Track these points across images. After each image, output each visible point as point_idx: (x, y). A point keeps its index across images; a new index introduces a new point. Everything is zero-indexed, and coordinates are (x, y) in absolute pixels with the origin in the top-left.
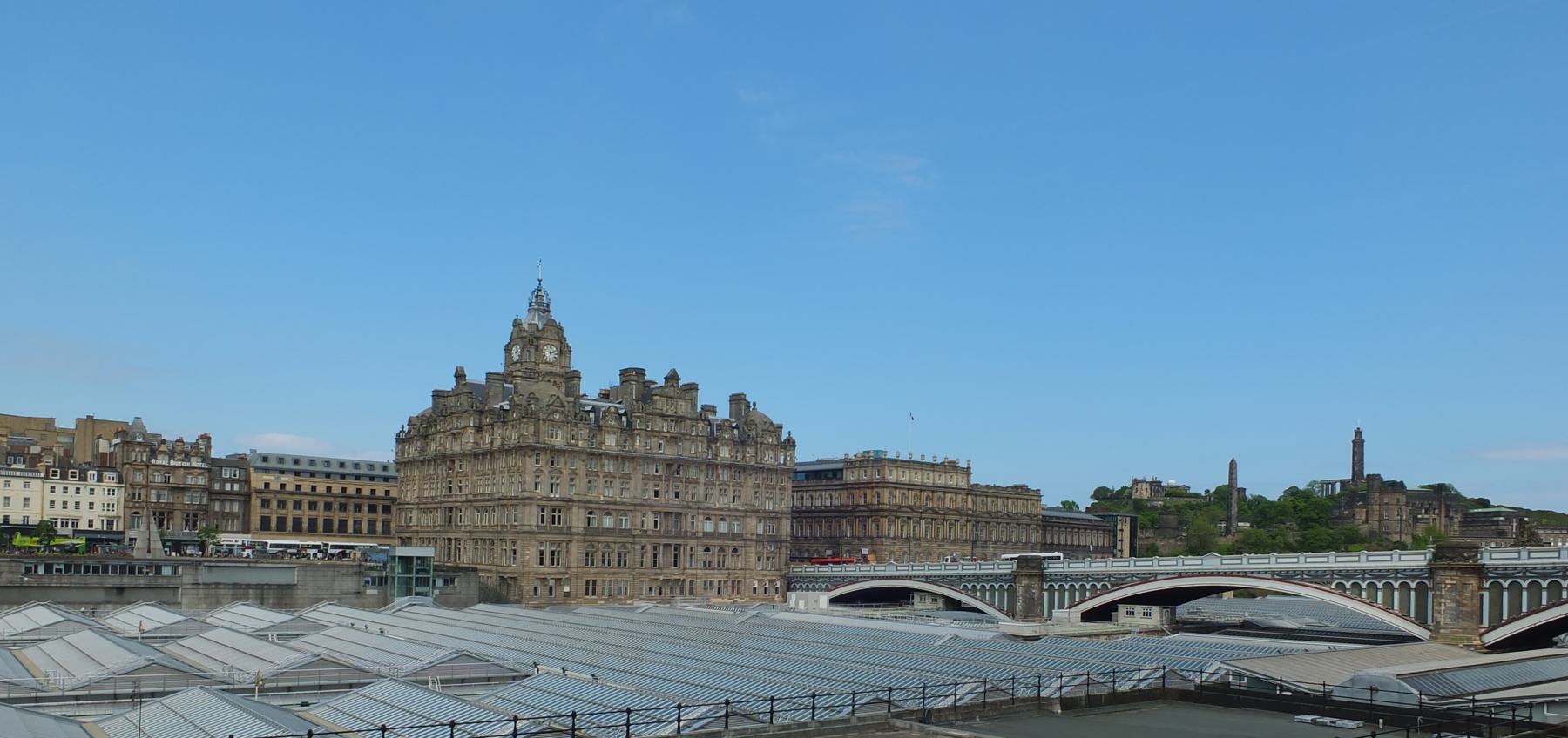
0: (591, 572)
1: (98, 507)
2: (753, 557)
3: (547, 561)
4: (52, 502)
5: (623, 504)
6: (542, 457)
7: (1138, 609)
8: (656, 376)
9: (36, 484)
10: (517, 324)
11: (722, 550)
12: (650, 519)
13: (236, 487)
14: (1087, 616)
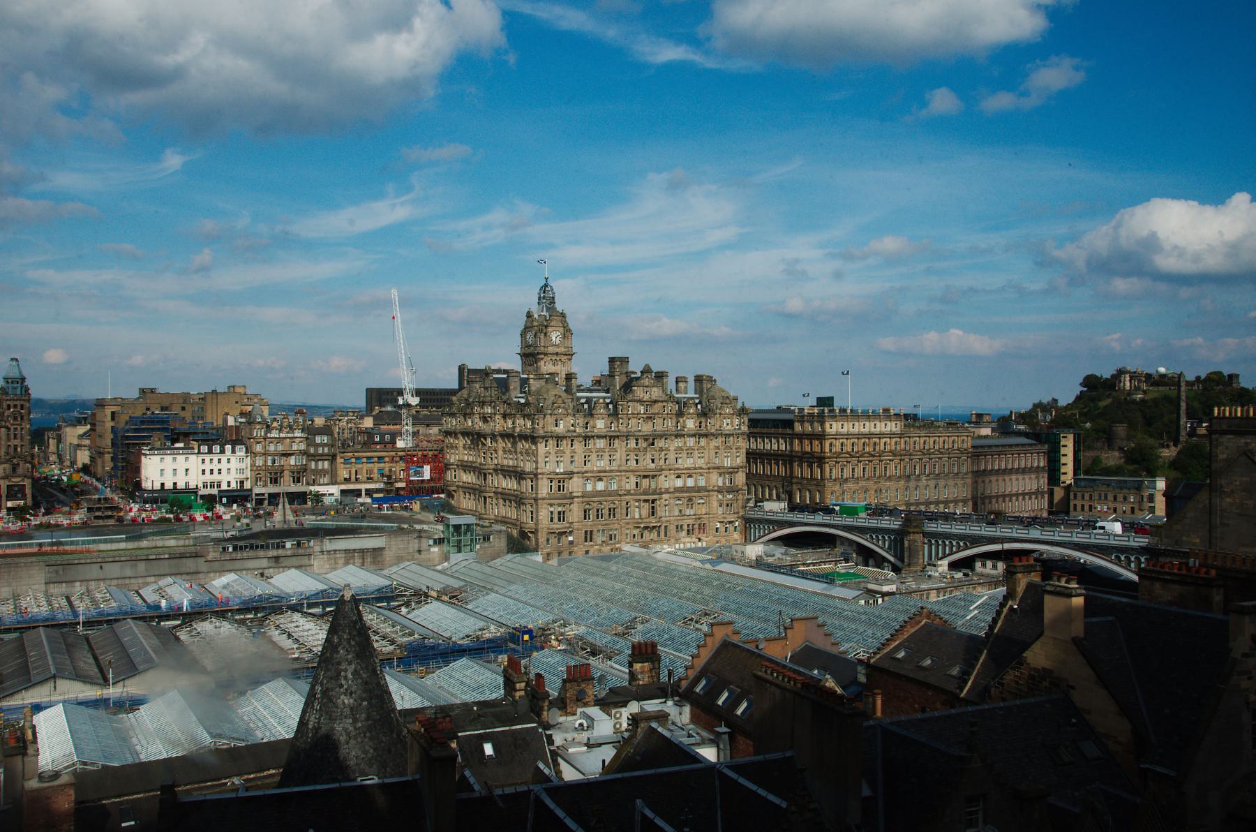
0: (588, 524)
1: (233, 471)
2: (715, 504)
3: (556, 520)
4: (204, 471)
5: (611, 471)
6: (550, 442)
7: (989, 564)
8: (635, 367)
9: (193, 458)
10: (529, 315)
11: (690, 499)
12: (633, 480)
13: (326, 450)
14: (954, 566)
